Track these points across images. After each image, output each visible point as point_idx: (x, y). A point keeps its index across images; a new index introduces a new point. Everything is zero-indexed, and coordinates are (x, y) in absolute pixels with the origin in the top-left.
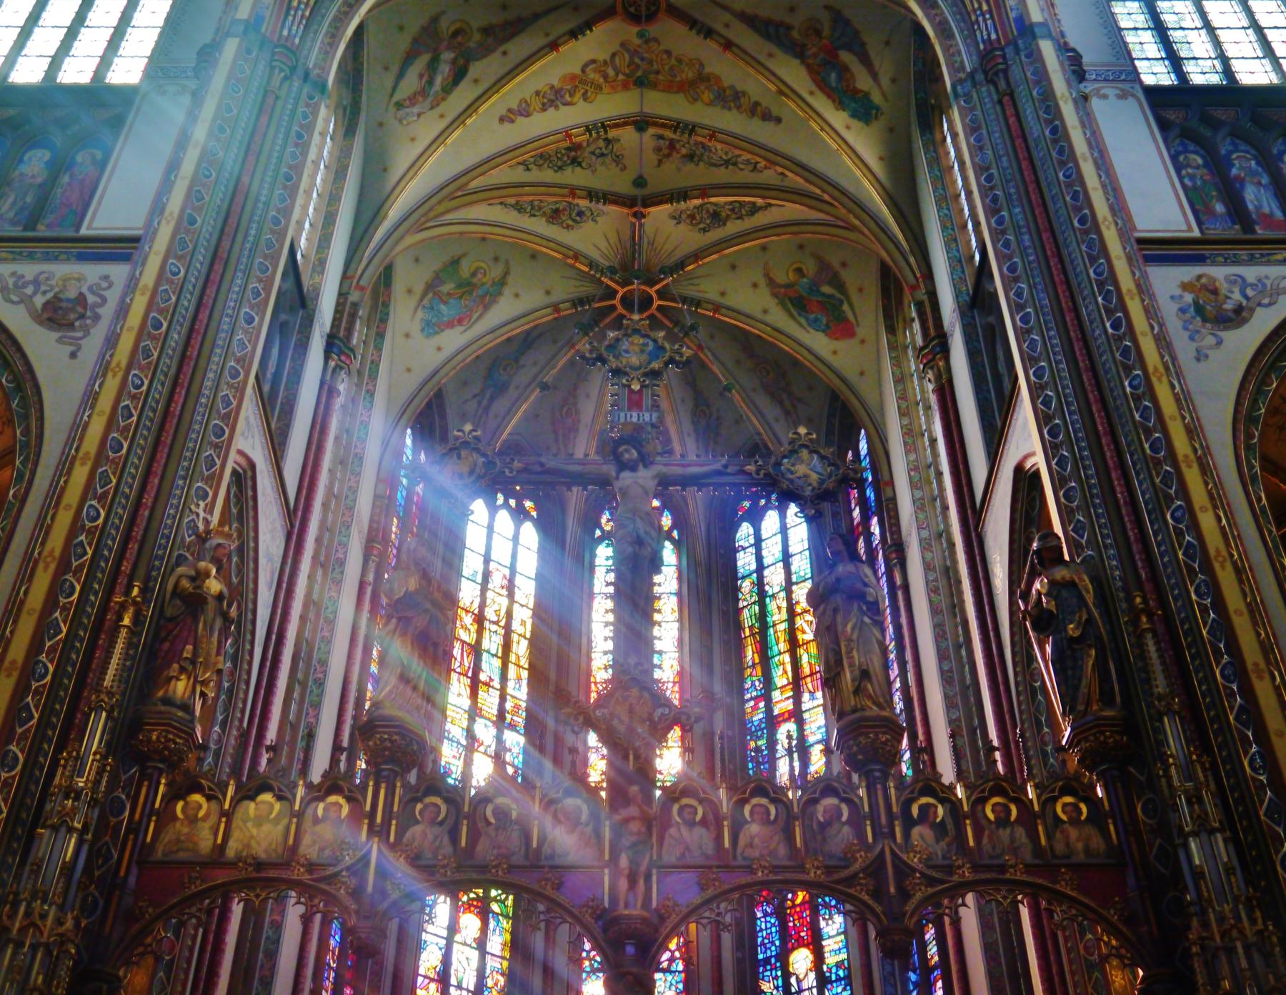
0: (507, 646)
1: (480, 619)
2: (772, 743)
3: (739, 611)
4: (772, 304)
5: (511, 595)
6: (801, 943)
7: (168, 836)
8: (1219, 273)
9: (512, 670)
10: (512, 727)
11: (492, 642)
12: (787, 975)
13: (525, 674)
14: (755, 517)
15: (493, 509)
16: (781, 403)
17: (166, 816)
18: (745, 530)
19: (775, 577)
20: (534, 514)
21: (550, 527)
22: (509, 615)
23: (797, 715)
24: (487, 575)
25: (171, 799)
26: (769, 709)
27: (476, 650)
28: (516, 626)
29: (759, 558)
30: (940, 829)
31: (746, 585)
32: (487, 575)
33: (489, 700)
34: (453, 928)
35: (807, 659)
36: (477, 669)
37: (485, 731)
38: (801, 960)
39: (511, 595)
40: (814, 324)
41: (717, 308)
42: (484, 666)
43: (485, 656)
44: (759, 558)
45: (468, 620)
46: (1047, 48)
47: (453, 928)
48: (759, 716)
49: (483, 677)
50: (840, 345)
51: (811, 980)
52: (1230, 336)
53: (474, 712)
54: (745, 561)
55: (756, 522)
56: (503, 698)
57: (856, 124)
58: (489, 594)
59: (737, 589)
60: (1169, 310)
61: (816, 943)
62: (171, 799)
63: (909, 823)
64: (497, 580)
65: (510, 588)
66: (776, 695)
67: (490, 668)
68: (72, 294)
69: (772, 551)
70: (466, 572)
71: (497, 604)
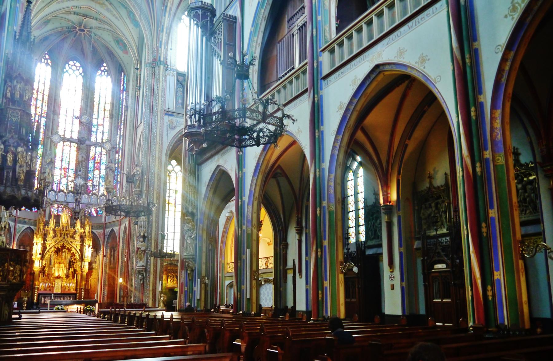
2: (97, 129)
4: (112, 40)
6: (97, 169)
8: (174, 119)
9: (44, 103)
12: (94, 174)
16: (110, 56)
23: (103, 125)
35: (107, 114)
38: (97, 172)
40: (120, 48)
41: (100, 37)
46: (162, 67)
50: (125, 55)
51: (98, 176)
52: (172, 131)
57: (134, 28)
60: (165, 124)
61: (100, 170)
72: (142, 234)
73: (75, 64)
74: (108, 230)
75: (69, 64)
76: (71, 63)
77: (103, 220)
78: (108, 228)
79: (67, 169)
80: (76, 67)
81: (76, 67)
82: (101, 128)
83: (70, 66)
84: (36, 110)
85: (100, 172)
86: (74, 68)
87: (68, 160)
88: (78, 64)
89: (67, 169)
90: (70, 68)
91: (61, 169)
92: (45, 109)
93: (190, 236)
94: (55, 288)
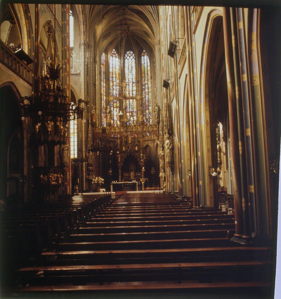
0: (116, 76)
1: (113, 73)
2: (145, 87)
3: (142, 69)
5: (116, 69)
6: (147, 109)
7: (96, 131)
10: (118, 86)
11: (114, 76)
12: (146, 113)
13: (118, 79)
14: (144, 56)
15: (112, 57)
17: (95, 130)
18: (143, 57)
19: (146, 65)
20: (117, 56)
21: (120, 58)
22: (116, 72)
23: (148, 84)
24: (113, 67)
25: (95, 129)
26: (145, 83)
27: (112, 77)
28: (117, 73)
29: (144, 62)
30: (146, 128)
31: (143, 65)
32: (113, 67)
33: (115, 83)
34: (114, 110)
36: (113, 80)
37: (114, 87)
38: (147, 111)
39: (116, 69)
42: (114, 79)
43: (113, 78)
44: (144, 62)
45: (111, 74)
47: (114, 110)
48: (144, 83)
49: (114, 81)
51: (148, 113)
53: (113, 85)
54: (143, 62)
55: (144, 57)
56: (116, 83)
58: (113, 70)
59: (142, 66)
62: (95, 129)
63: (144, 128)
64: (114, 67)
65: (115, 68)
66: (146, 81)
67: (114, 79)
68: (76, 81)
69: (146, 62)
70: (110, 67)
71: (114, 70)
72: (161, 146)
73: (130, 52)
74: (155, 143)
75: (127, 54)
76: (128, 52)
77: (153, 138)
78: (156, 142)
79: (132, 112)
80: (131, 54)
81: (131, 54)
82: (147, 86)
83: (128, 55)
84: (113, 83)
85: (149, 111)
86: (130, 55)
87: (132, 107)
88: (131, 52)
89: (132, 112)
90: (128, 56)
91: (129, 113)
92: (118, 81)
93: (169, 148)
94: (131, 176)
